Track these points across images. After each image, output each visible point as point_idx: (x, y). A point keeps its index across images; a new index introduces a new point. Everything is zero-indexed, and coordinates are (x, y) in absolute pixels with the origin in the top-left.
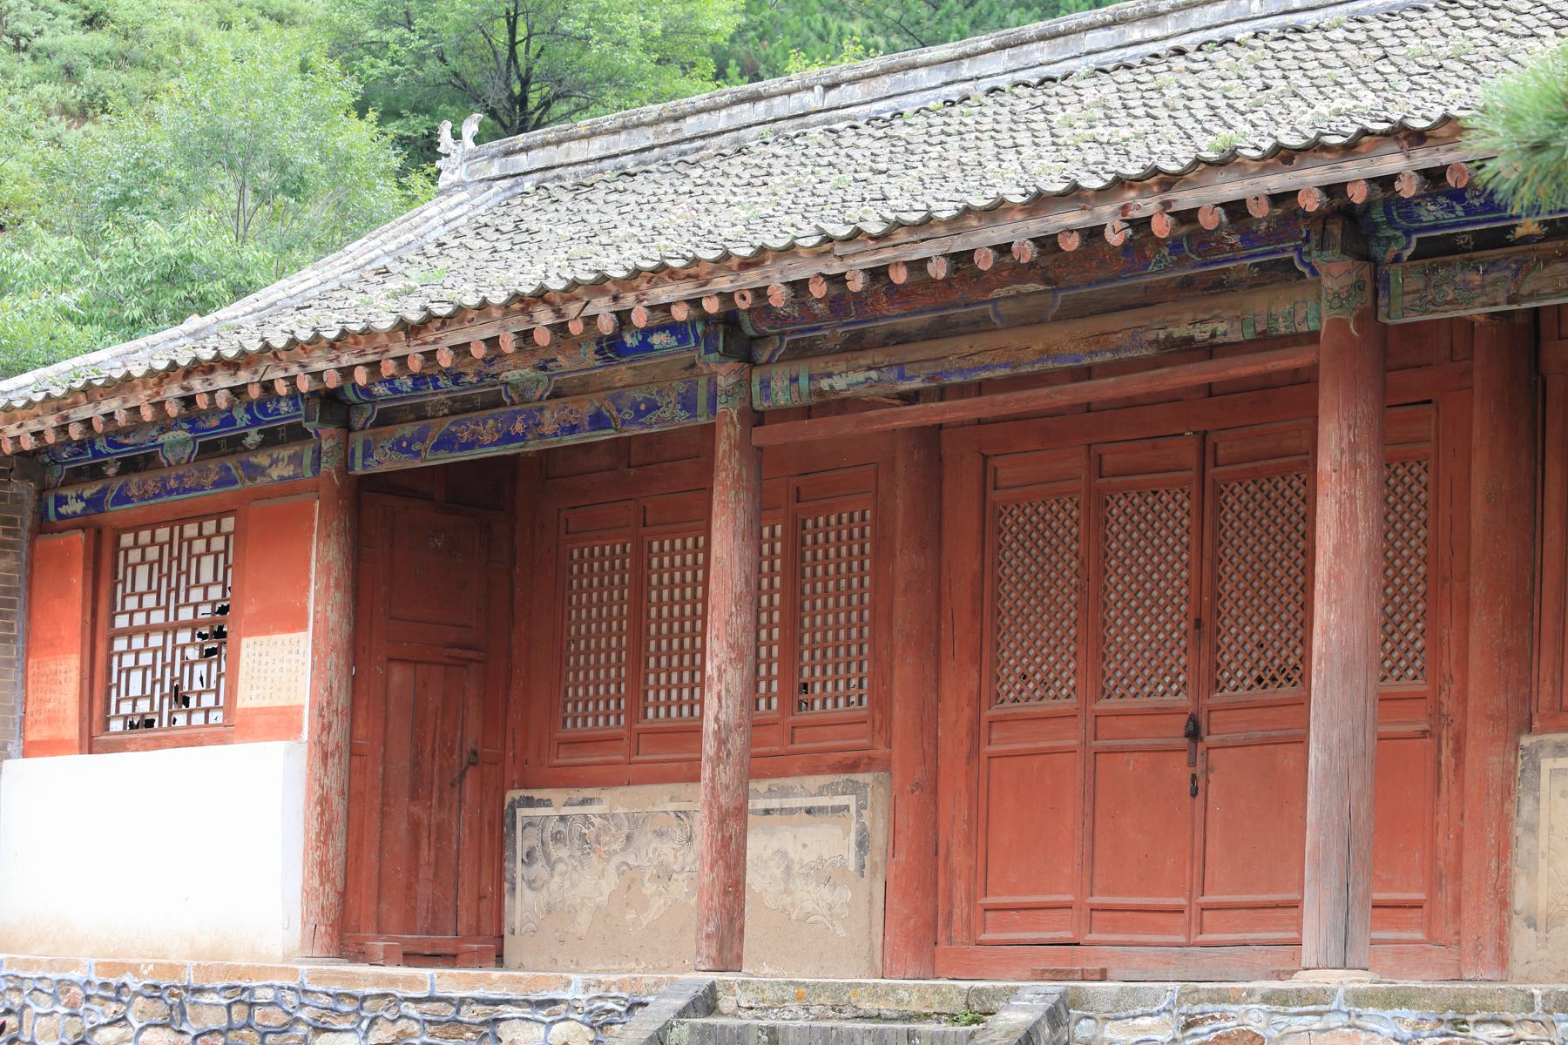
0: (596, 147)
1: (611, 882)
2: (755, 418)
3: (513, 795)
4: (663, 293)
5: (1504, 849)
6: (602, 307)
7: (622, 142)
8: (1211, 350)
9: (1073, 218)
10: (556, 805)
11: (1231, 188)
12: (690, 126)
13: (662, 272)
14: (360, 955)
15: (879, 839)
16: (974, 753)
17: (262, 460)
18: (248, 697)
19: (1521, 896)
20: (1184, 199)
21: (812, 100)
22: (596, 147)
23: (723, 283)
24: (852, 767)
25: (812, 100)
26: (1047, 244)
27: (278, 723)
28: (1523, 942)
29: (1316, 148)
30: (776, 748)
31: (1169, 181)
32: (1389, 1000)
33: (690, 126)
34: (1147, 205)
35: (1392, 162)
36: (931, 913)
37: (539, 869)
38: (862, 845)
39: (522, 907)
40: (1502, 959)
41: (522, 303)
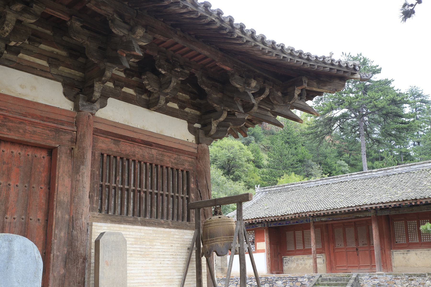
0: (275, 189)
1: (295, 265)
2: (314, 222)
3: (283, 257)
4: (310, 213)
5: (391, 260)
6: (304, 214)
7: (278, 188)
8: (361, 217)
9: (351, 208)
10: (288, 258)
11: (366, 207)
12: (286, 187)
13: (310, 212)
14: (273, 273)
15: (325, 260)
16: (334, 252)
17: (257, 225)
18: (258, 249)
19: (393, 265)
20: (362, 207)
21: (300, 185)
22: (275, 189)
23: (316, 213)
24: (321, 253)
25: (300, 185)
26: (349, 210)
27: (262, 251)
28: (394, 269)
29: (374, 204)
30: (319, 252)
31: (360, 206)
32: (389, 274)
33: (286, 187)
34: (359, 208)
35: (381, 205)
36: (331, 267)
37: (287, 264)
38: (323, 261)
39: (285, 268)
40: (392, 270)
41: (295, 214)
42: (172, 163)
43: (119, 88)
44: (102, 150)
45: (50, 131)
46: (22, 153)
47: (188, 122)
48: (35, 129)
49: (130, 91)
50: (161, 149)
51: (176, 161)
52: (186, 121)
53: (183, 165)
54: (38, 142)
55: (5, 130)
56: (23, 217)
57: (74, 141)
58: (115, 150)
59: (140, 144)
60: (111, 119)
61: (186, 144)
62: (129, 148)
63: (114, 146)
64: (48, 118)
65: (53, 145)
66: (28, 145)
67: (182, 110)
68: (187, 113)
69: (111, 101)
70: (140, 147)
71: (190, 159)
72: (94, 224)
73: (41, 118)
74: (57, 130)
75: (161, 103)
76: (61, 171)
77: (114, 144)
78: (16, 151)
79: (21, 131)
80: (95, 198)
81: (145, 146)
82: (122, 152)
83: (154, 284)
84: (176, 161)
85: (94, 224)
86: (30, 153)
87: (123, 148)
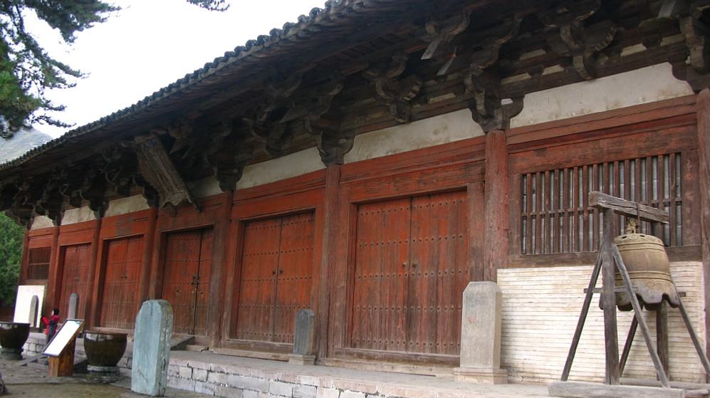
42: (640, 149)
43: (536, 75)
44: (522, 169)
45: (460, 170)
46: (449, 201)
47: (670, 62)
48: (445, 174)
49: (557, 69)
50: (614, 135)
51: (648, 143)
52: (667, 63)
53: (666, 144)
54: (453, 187)
55: (422, 185)
56: (453, 270)
57: (483, 173)
58: (540, 164)
59: (576, 141)
60: (532, 123)
61: (668, 104)
62: (561, 153)
63: (538, 158)
64: (458, 156)
65: (463, 185)
66: (453, 192)
67: (653, 48)
68: (666, 47)
69: (529, 99)
70: (578, 145)
71: (684, 128)
72: (499, 271)
73: (452, 159)
74: (467, 165)
75: (579, 68)
76: (472, 213)
77: (538, 156)
78: (443, 201)
79: (434, 181)
80: (516, 236)
81: (586, 140)
82: (551, 163)
83: (584, 351)
84: (648, 143)
85: (499, 271)
86: (455, 200)
87: (551, 156)
